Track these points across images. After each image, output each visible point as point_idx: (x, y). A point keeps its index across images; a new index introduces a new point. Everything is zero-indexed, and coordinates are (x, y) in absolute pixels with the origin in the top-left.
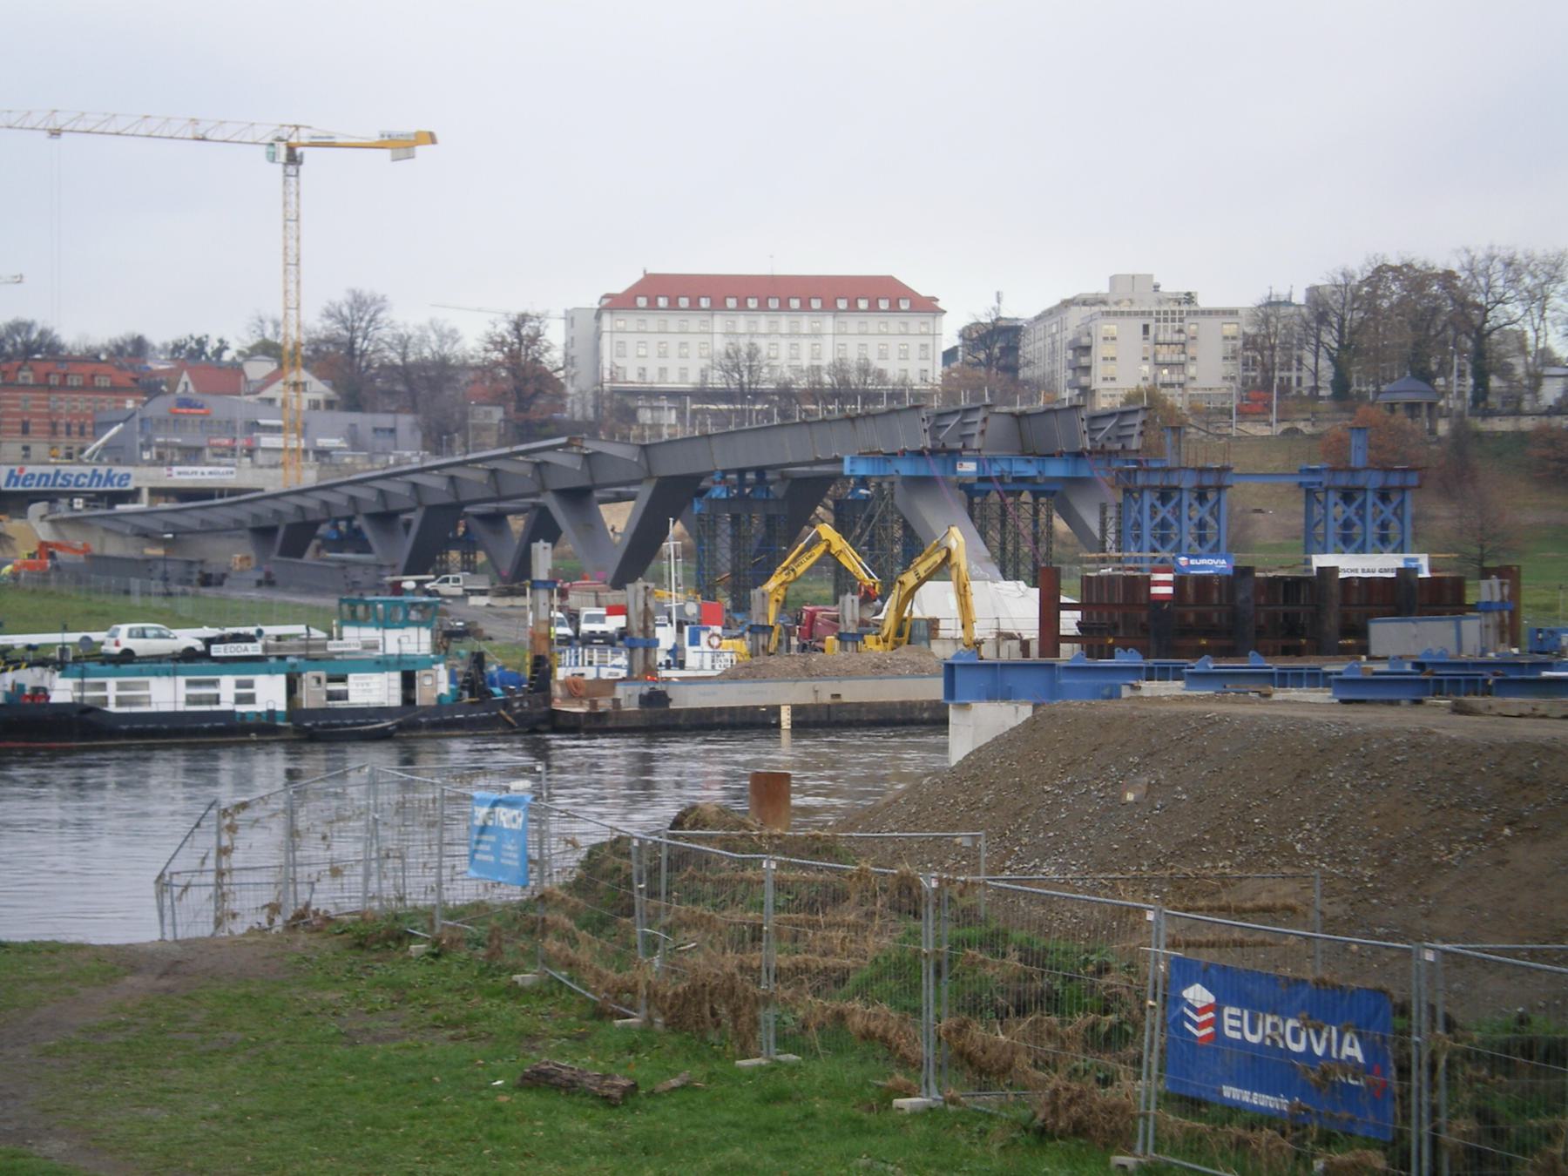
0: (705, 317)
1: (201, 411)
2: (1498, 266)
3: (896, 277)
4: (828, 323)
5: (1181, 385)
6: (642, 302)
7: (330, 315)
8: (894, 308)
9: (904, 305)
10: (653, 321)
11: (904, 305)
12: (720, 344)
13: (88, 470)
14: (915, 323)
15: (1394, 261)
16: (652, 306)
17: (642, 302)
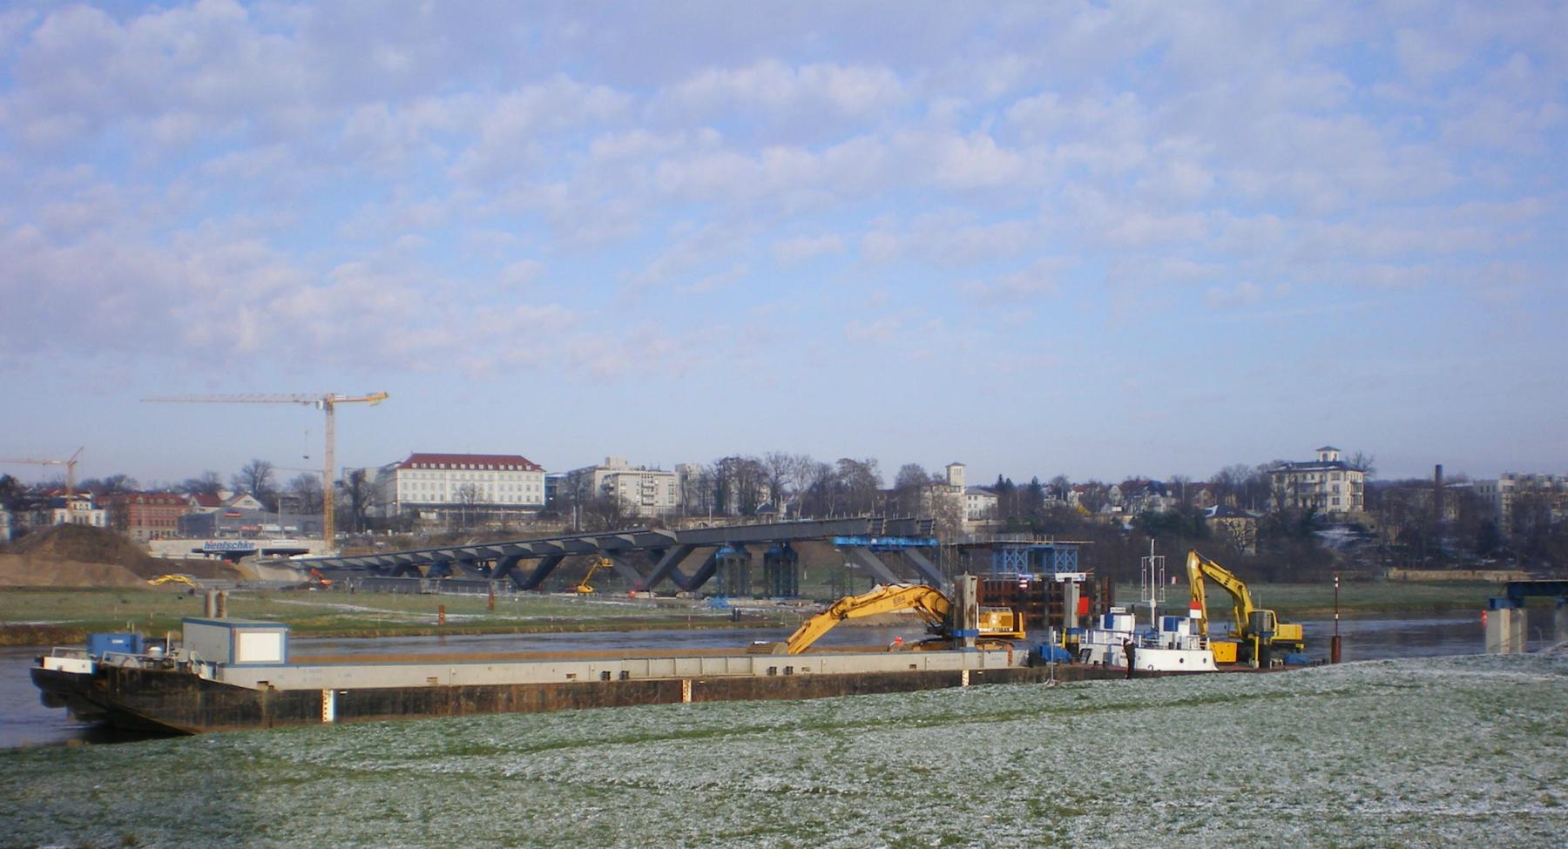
0: (443, 472)
1: (237, 515)
3: (523, 456)
4: (496, 474)
5: (652, 505)
6: (415, 465)
7: (246, 472)
8: (524, 469)
9: (529, 468)
10: (419, 473)
11: (529, 468)
12: (458, 485)
13: (237, 542)
14: (533, 475)
15: (731, 457)
16: (419, 467)
17: (415, 465)
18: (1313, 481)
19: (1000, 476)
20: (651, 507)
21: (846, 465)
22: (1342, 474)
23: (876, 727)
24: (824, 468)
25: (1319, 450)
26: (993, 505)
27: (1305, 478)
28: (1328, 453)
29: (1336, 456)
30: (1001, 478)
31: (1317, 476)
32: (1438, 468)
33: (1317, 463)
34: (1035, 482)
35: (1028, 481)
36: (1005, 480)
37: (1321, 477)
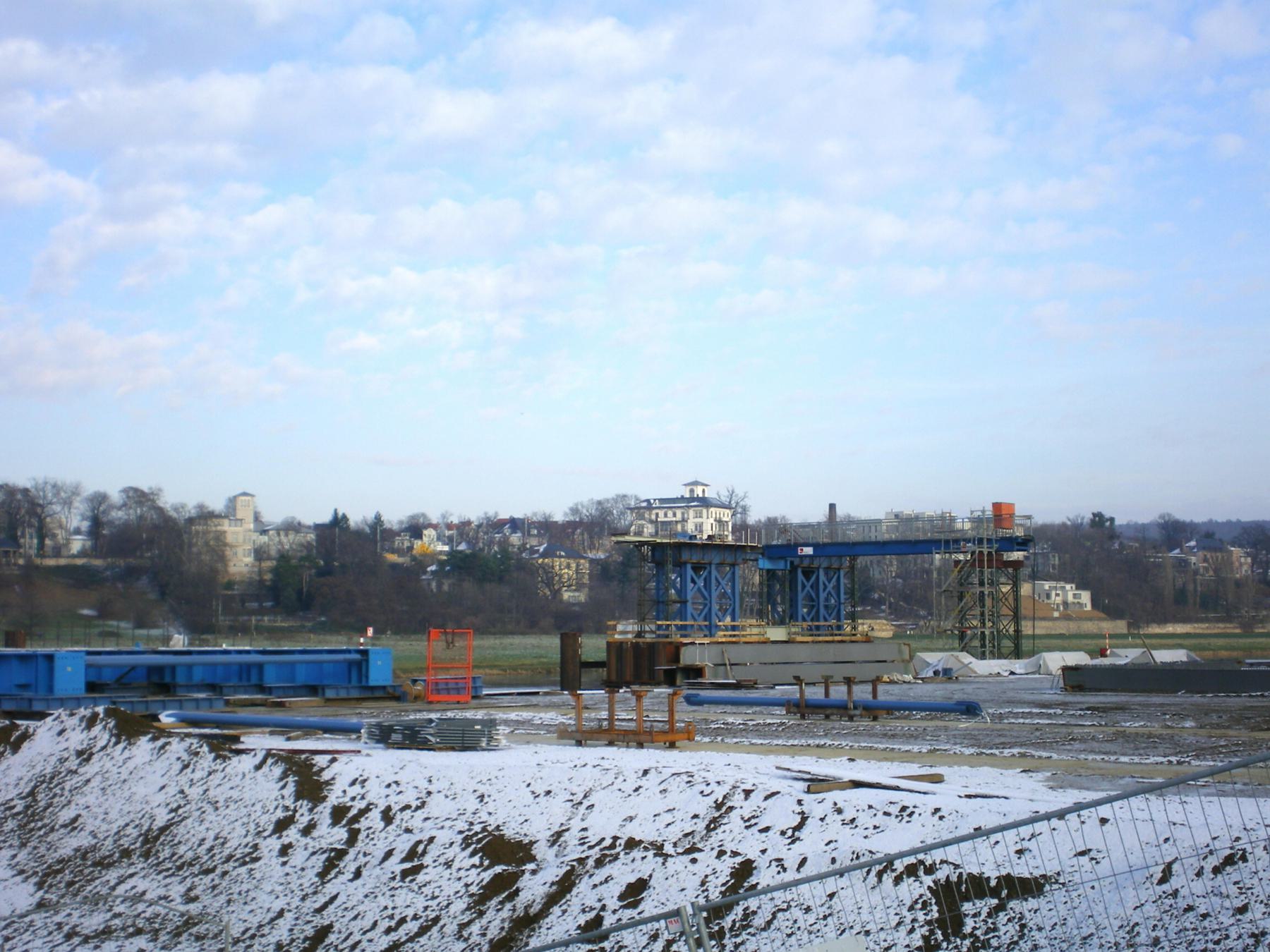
2: (49, 487)
18: (674, 519)
19: (336, 510)
21: (131, 494)
22: (705, 511)
24: (99, 500)
25: (685, 485)
27: (666, 515)
28: (695, 488)
29: (704, 491)
32: (832, 507)
33: (682, 499)
37: (683, 514)
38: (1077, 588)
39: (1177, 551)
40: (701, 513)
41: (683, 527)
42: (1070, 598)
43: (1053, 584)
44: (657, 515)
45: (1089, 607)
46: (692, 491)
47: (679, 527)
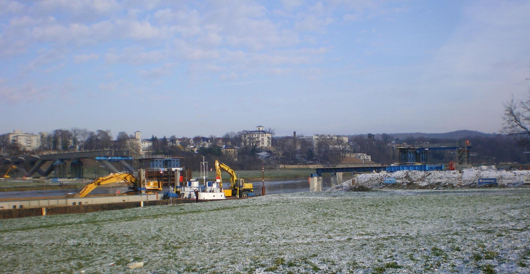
5: (30, 146)
20: (30, 147)
22: (264, 135)
23: (111, 222)
24: (92, 133)
25: (257, 127)
26: (151, 145)
27: (253, 136)
30: (153, 136)
31: (257, 135)
32: (295, 133)
33: (257, 131)
34: (165, 137)
35: (163, 137)
36: (154, 137)
37: (258, 135)
38: (367, 155)
39: (390, 144)
40: (263, 135)
41: (258, 139)
42: (366, 158)
43: (362, 154)
44: (250, 136)
45: (370, 160)
46: (259, 129)
47: (257, 139)
